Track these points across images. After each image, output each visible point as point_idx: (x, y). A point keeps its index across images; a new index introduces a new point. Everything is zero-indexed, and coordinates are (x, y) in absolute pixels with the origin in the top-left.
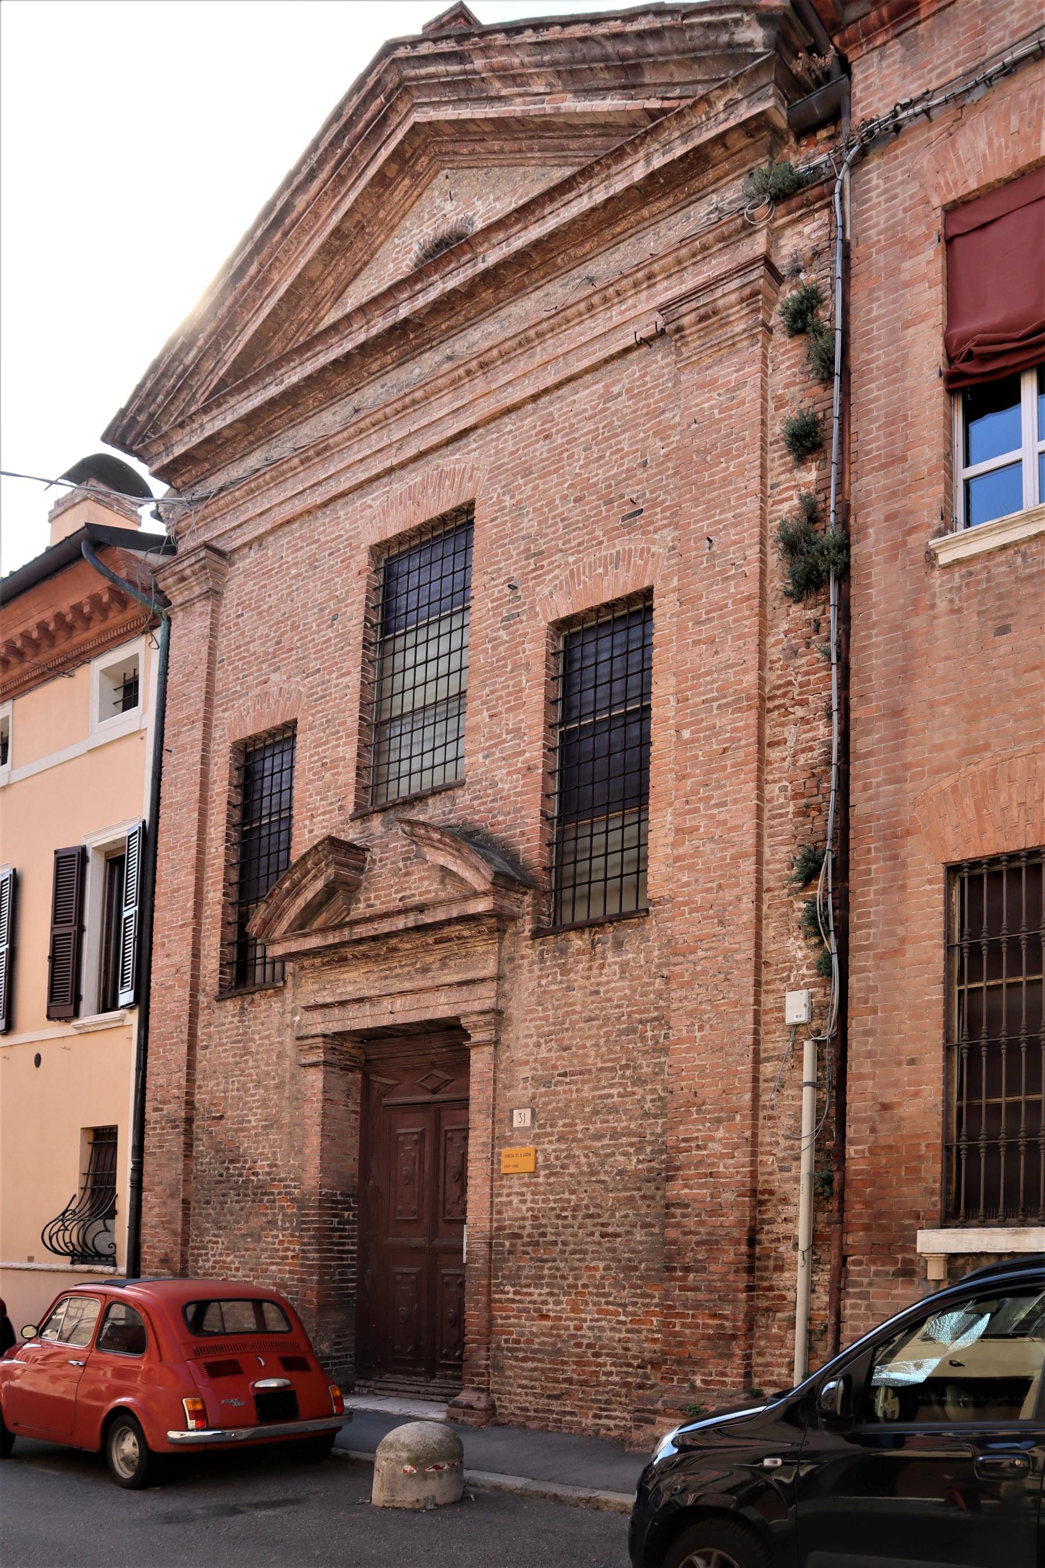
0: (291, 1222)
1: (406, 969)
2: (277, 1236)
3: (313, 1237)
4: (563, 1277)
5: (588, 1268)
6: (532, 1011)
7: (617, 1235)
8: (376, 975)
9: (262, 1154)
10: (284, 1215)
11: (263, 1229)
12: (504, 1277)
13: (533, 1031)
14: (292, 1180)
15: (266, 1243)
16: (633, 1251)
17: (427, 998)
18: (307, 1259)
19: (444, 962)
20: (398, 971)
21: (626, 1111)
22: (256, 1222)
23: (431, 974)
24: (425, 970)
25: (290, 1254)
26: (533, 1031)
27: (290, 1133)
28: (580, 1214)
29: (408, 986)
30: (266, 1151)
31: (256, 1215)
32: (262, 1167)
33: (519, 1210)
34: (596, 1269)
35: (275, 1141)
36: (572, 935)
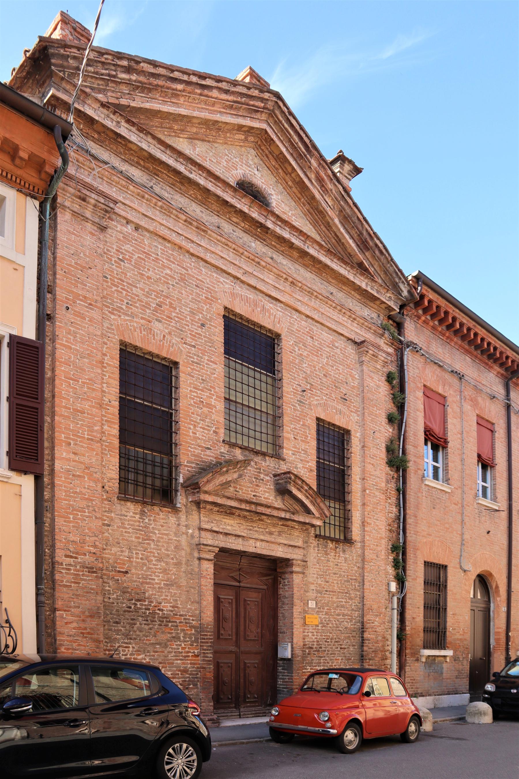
0: (190, 638)
1: (261, 530)
2: (180, 645)
3: (210, 646)
4: (328, 663)
5: (336, 659)
6: (315, 565)
7: (345, 648)
8: (245, 527)
9: (164, 599)
10: (185, 634)
11: (168, 641)
12: (306, 663)
13: (315, 572)
14: (189, 616)
15: (172, 648)
16: (350, 654)
17: (273, 547)
18: (207, 657)
19: (280, 533)
20: (256, 529)
21: (347, 608)
22: (162, 637)
23: (273, 536)
24: (271, 533)
25: (190, 654)
26: (315, 572)
27: (188, 591)
28: (333, 641)
29: (262, 537)
30: (168, 598)
31: (163, 633)
32: (167, 607)
33: (312, 638)
34: (338, 660)
35: (175, 594)
36: (329, 541)
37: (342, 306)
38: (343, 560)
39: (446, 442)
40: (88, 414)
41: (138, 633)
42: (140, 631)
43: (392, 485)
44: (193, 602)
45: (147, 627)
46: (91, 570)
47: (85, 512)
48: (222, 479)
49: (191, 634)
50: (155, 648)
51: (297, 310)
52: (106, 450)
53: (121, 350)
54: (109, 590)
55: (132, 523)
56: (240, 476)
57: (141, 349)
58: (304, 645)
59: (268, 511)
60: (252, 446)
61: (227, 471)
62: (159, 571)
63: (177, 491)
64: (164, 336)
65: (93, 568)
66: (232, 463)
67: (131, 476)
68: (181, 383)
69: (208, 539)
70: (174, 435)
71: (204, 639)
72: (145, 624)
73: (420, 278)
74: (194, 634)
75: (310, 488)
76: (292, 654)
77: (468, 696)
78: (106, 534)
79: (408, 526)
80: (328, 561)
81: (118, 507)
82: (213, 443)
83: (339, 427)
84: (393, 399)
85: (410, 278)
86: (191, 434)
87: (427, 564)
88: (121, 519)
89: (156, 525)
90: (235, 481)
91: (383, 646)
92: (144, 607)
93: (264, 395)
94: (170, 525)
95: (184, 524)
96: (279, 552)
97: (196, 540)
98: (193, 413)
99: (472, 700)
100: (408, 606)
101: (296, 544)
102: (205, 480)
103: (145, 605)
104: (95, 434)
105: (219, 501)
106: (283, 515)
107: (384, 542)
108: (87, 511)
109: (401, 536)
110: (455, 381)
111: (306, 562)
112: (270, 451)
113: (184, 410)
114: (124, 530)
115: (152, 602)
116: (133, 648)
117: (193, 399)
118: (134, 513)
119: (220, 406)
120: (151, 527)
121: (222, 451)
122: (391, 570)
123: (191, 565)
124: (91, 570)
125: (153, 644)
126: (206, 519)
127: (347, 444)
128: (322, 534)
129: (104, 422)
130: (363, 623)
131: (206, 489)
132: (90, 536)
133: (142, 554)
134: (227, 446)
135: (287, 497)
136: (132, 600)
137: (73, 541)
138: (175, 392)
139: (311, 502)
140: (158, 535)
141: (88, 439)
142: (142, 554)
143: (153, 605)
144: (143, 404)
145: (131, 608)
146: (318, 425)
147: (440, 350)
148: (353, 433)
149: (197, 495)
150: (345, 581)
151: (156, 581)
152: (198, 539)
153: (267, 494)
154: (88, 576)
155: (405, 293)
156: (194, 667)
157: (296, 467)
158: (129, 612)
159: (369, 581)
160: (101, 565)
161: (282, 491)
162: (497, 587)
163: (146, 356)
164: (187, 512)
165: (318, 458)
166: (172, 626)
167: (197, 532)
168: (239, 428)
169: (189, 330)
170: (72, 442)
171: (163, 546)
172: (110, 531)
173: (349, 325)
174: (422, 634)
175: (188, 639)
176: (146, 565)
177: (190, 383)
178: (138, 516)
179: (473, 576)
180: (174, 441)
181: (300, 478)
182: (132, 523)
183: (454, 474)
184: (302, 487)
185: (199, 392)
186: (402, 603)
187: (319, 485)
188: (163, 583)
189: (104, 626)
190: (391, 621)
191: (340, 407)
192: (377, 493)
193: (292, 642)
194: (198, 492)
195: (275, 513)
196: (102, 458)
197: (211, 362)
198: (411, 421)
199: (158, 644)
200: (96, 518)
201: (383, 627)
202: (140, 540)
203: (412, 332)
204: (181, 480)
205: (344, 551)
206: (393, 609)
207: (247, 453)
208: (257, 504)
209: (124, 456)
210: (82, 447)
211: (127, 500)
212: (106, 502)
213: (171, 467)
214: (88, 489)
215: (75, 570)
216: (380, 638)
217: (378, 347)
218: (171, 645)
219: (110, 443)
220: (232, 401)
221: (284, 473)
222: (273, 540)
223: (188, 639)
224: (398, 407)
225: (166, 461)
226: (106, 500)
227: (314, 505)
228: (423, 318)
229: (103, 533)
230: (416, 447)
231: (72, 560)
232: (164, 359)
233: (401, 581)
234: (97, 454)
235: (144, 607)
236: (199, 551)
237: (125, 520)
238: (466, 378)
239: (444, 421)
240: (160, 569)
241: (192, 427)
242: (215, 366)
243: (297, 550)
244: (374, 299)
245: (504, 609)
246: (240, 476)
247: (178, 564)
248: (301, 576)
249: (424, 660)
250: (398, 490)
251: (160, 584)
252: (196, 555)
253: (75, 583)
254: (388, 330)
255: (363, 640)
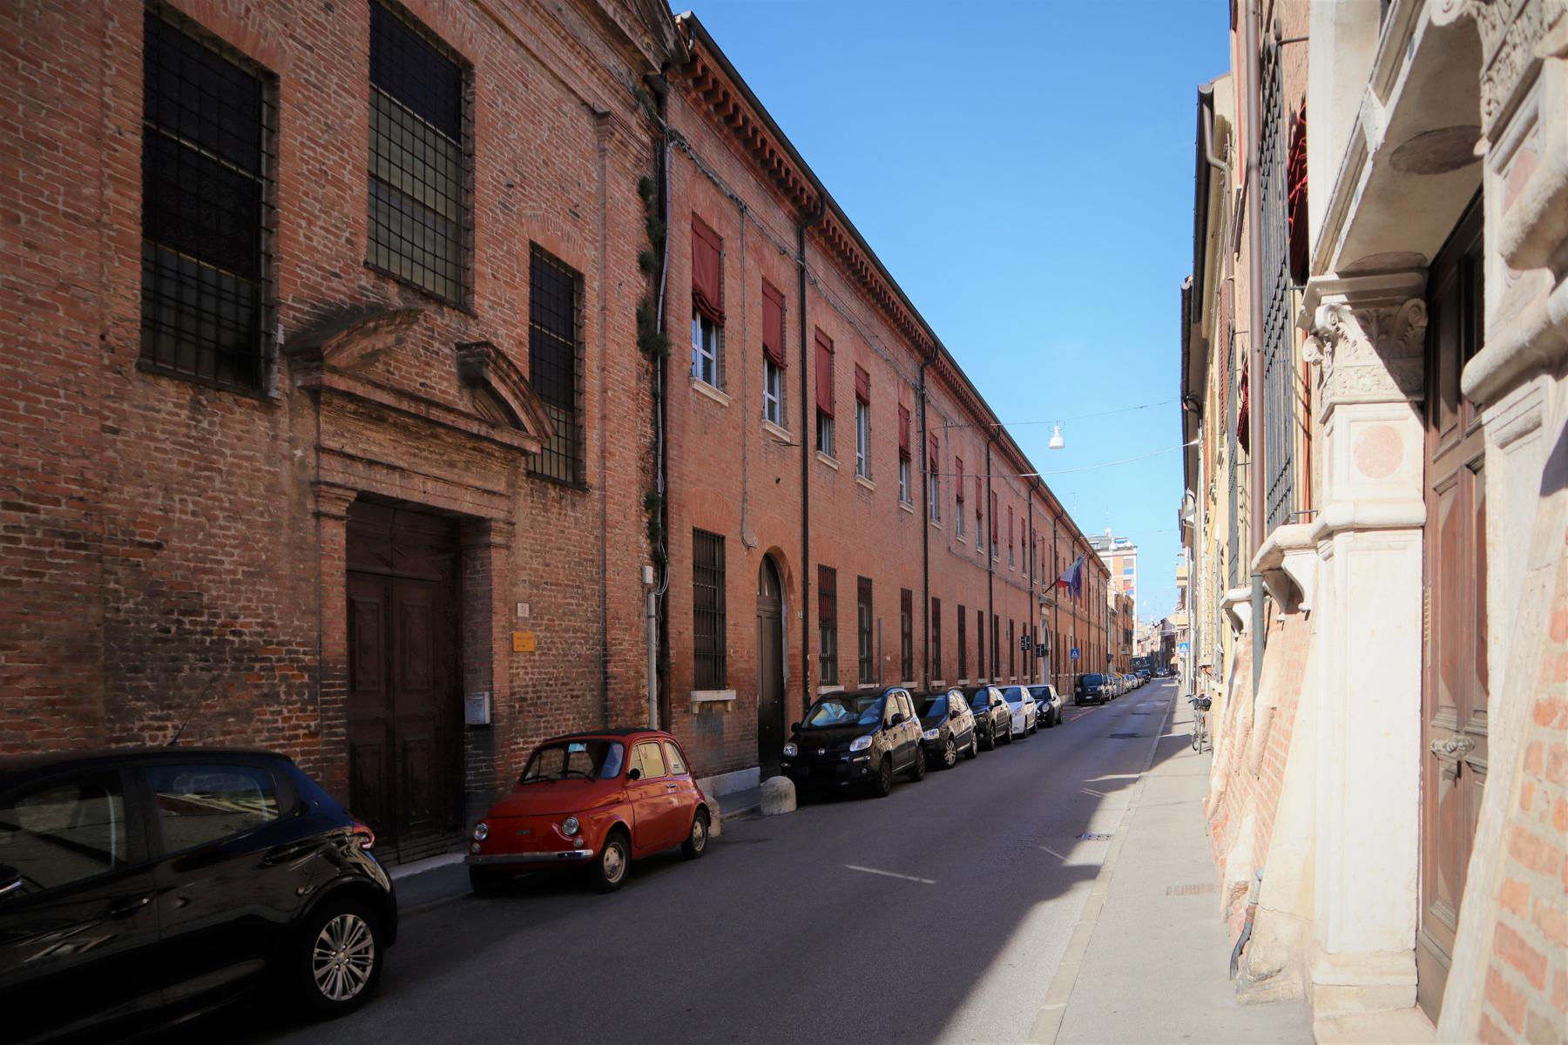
0: (301, 694)
1: (435, 456)
2: (280, 712)
3: (341, 710)
9: (244, 608)
10: (289, 686)
11: (254, 704)
14: (299, 644)
15: (262, 721)
17: (457, 492)
18: (336, 735)
20: (425, 454)
22: (240, 697)
24: (451, 464)
25: (301, 732)
27: (293, 588)
29: (436, 472)
32: (248, 625)
35: (268, 594)
37: (576, 39)
38: (570, 523)
39: (722, 317)
40: (66, 152)
41: (186, 691)
42: (192, 687)
43: (646, 385)
44: (304, 613)
45: (206, 676)
46: (73, 540)
47: (57, 396)
48: (363, 345)
49: (302, 686)
50: (225, 724)
51: (502, 26)
52: (109, 247)
53: (147, 14)
54: (116, 591)
55: (172, 428)
56: (400, 341)
57: (195, 24)
58: (512, 694)
59: (449, 419)
60: (418, 280)
61: (376, 329)
62: (233, 542)
63: (270, 361)
64: (248, 10)
65: (77, 536)
66: (380, 313)
67: (168, 316)
68: (282, 122)
69: (335, 472)
70: (264, 235)
71: (328, 694)
72: (202, 669)
73: (692, 24)
74: (307, 686)
75: (522, 378)
76: (492, 715)
77: (757, 770)
78: (110, 453)
79: (669, 463)
80: (548, 523)
81: (139, 388)
82: (346, 264)
83: (566, 266)
84: (647, 227)
85: (678, 20)
86: (302, 239)
87: (698, 534)
88: (145, 418)
89: (225, 435)
90: (387, 351)
91: (637, 688)
92: (199, 629)
93: (441, 179)
94: (257, 438)
95: (286, 435)
96: (467, 504)
97: (310, 474)
98: (306, 194)
99: (764, 777)
100: (672, 612)
101: (496, 489)
102: (334, 342)
103: (202, 623)
104: (84, 205)
105: (360, 390)
106: (475, 428)
107: (634, 489)
108: (62, 392)
109: (659, 481)
110: (735, 214)
111: (513, 524)
112: (450, 297)
113: (288, 185)
114: (152, 445)
115: (217, 616)
116: (175, 727)
117: (307, 163)
118: (177, 405)
119: (361, 188)
120: (215, 439)
121: (363, 283)
122: (644, 543)
123: (300, 529)
124: (73, 540)
125: (221, 714)
126: (331, 429)
127: (579, 300)
128: (539, 470)
129: (105, 180)
130: (605, 644)
131: (334, 362)
132: (70, 457)
133: (195, 503)
134: (372, 275)
135: (480, 392)
136: (172, 612)
137: (26, 468)
138: (269, 139)
139: (523, 406)
140: (230, 459)
141: (66, 215)
142: (195, 503)
143: (218, 622)
144: (198, 153)
145: (168, 631)
146: (532, 256)
147: (715, 155)
148: (587, 279)
149: (315, 374)
150: (577, 564)
151: (227, 566)
152: (313, 472)
153: (445, 384)
154: (64, 556)
155: (671, 45)
156: (308, 761)
157: (495, 334)
158: (165, 641)
159: (614, 564)
160: (97, 529)
161: (472, 380)
162: (790, 576)
163: (207, 45)
164: (291, 410)
165: (532, 320)
166: (262, 669)
167: (312, 455)
168: (395, 240)
169: (301, 10)
170: (22, 215)
171: (241, 485)
172: (120, 445)
173: (584, 77)
174: (692, 663)
175: (295, 697)
176: (203, 528)
177: (302, 127)
178: (184, 413)
179: (759, 558)
180: (263, 248)
181: (505, 358)
182: (172, 428)
183: (732, 376)
184: (508, 376)
185: (319, 150)
186: (663, 604)
187: (532, 372)
188: (240, 569)
189: (107, 679)
190: (647, 640)
191: (568, 227)
192: (624, 399)
193: (491, 689)
194: (317, 368)
195: (461, 423)
196: (102, 267)
197: (345, 90)
198: (674, 273)
199: (232, 714)
200: (86, 411)
201: (635, 652)
202: (191, 470)
203: (678, 115)
204: (280, 338)
205: (574, 505)
206: (650, 617)
207: (409, 294)
208: (431, 403)
209: (153, 270)
210: (51, 231)
211: (161, 373)
212: (109, 375)
213: (259, 307)
214: (66, 338)
215: (29, 542)
216: (632, 673)
217: (628, 129)
218: (259, 714)
219: (120, 232)
220: (382, 181)
221: (479, 344)
222: (456, 478)
223: (295, 697)
224: (655, 244)
225: (245, 290)
226: (108, 368)
227: (527, 412)
228: (694, 94)
229: (103, 450)
230: (680, 320)
231: (22, 515)
232: (248, 60)
233: (660, 562)
234: (88, 256)
235: (199, 629)
236: (318, 497)
237: (156, 420)
238: (750, 212)
239: (720, 282)
240: (235, 538)
241: (303, 223)
242: (351, 101)
243: (496, 501)
244: (623, 40)
245: (800, 614)
246: (400, 341)
247: (274, 527)
248: (504, 552)
249: (696, 710)
250: (654, 395)
251: (234, 572)
252: (310, 506)
253: (31, 574)
254: (645, 103)
255: (606, 678)
